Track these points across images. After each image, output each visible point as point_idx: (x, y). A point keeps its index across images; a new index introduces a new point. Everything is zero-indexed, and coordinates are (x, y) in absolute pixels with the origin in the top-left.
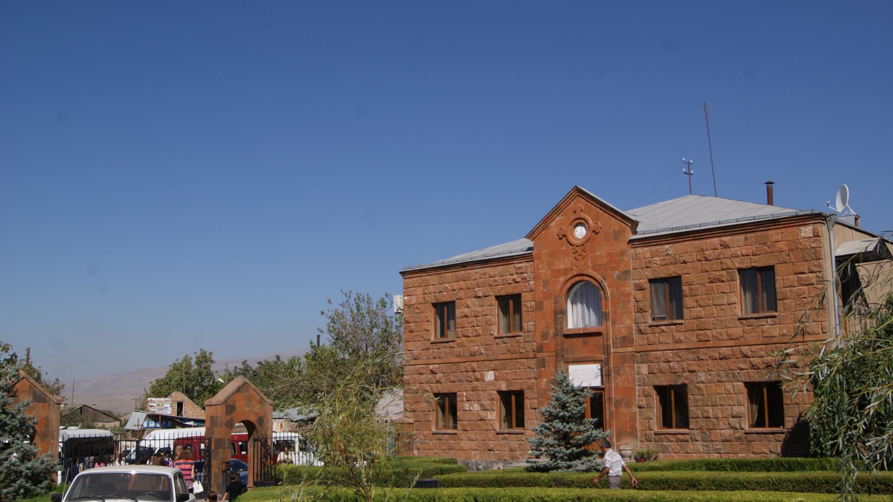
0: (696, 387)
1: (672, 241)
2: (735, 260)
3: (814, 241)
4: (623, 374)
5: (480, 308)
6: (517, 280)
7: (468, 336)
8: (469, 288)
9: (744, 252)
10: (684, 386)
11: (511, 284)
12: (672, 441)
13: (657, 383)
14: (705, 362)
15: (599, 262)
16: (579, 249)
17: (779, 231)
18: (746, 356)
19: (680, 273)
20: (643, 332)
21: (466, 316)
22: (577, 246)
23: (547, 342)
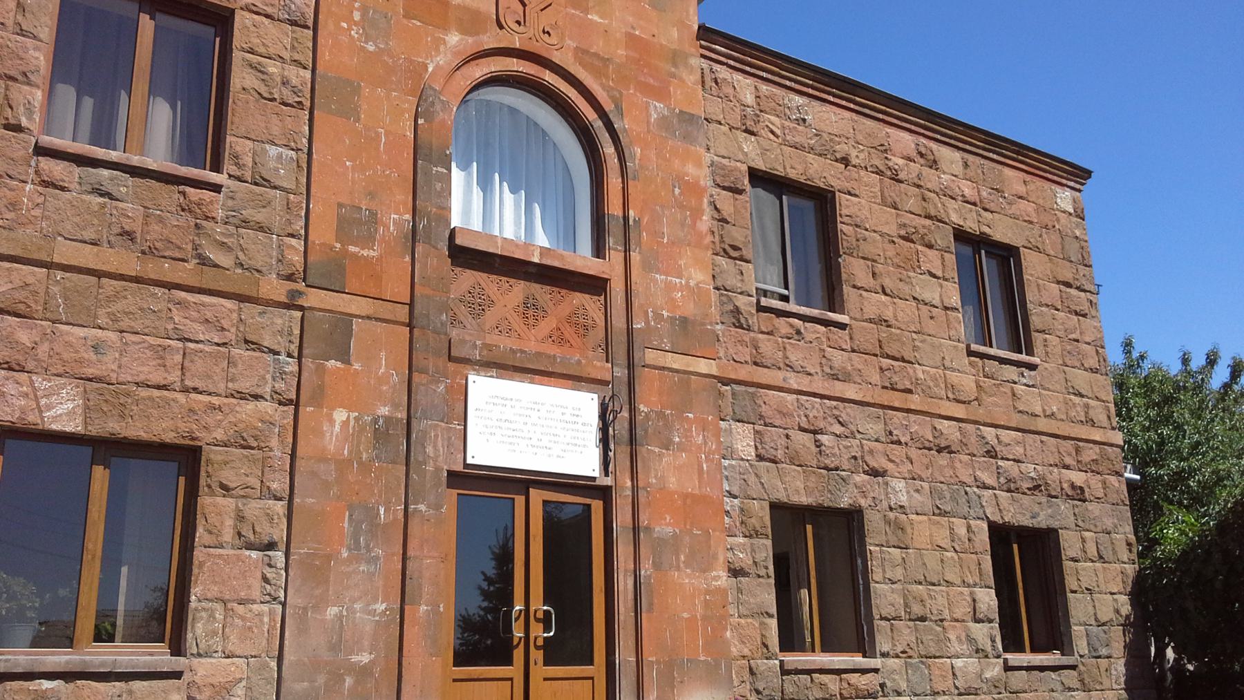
0: (888, 522)
1: (810, 91)
2: (951, 204)
4: (681, 448)
9: (967, 192)
10: (851, 520)
13: (781, 496)
15: (598, 46)
17: (1022, 174)
18: (991, 454)
19: (836, 184)
20: (743, 321)
23: (372, 253)
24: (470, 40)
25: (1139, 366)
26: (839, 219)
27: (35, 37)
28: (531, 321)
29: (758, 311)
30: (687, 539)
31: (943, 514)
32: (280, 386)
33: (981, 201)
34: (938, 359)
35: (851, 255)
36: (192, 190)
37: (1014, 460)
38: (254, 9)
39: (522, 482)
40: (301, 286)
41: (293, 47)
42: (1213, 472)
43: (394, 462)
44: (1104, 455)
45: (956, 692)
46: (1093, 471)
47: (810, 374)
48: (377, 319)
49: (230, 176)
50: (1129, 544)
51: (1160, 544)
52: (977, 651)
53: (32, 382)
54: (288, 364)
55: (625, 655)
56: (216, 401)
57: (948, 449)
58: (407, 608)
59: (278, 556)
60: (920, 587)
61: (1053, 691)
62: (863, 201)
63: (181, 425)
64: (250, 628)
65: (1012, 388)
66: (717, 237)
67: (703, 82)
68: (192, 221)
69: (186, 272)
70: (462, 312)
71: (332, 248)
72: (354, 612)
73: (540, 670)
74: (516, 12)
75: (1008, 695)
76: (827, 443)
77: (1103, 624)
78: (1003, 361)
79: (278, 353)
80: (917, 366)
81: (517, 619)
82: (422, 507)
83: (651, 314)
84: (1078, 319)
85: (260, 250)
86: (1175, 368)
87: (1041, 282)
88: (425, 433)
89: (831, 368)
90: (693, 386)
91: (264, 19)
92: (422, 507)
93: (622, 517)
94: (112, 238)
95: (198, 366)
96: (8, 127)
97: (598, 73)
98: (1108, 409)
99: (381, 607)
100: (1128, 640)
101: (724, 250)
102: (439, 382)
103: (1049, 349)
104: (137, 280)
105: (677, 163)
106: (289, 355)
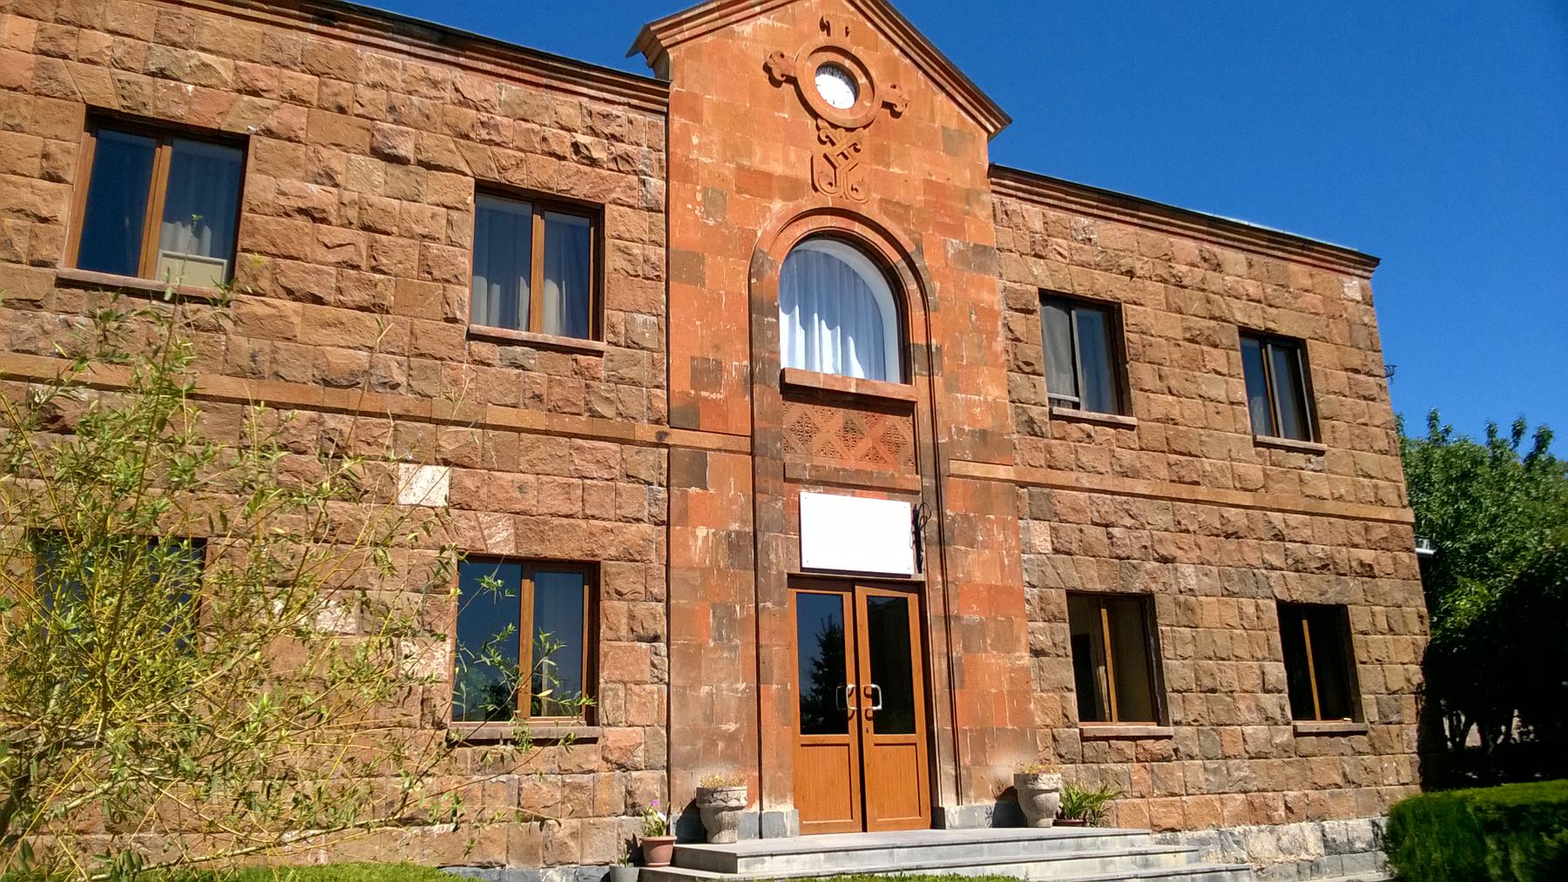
0: (1178, 604)
1: (1095, 211)
2: (1235, 304)
3: (1366, 312)
4: (984, 546)
5: (396, 202)
6: (595, 155)
7: (318, 300)
8: (342, 110)
9: (1252, 291)
10: (1144, 604)
11: (562, 158)
12: (1128, 760)
14: (1192, 537)
15: (900, 195)
16: (843, 141)
17: (1307, 269)
18: (1279, 537)
19: (1121, 295)
20: (1037, 429)
21: (315, 216)
22: (835, 126)
23: (719, 396)
24: (791, 205)
25: (1444, 440)
26: (1125, 327)
27: (461, 246)
28: (851, 443)
29: (1050, 419)
30: (992, 625)
31: (1232, 594)
32: (655, 510)
33: (1266, 298)
34: (1225, 451)
35: (1137, 360)
36: (582, 357)
37: (1302, 542)
38: (620, 202)
39: (848, 581)
40: (666, 428)
41: (651, 230)
42: (1509, 544)
43: (745, 568)
44: (1392, 532)
45: (1247, 756)
46: (1383, 549)
47: (1101, 474)
48: (725, 451)
49: (609, 342)
50: (1421, 617)
51: (1452, 616)
52: (1267, 719)
53: (477, 518)
54: (660, 492)
55: (942, 724)
56: (608, 525)
57: (1235, 535)
58: (762, 686)
59: (662, 646)
60: (1210, 662)
61: (1343, 754)
62: (1149, 309)
63: (585, 545)
64: (645, 703)
65: (1299, 474)
66: (1011, 357)
67: (995, 215)
68: (583, 382)
69: (581, 424)
70: (794, 439)
71: (688, 394)
72: (722, 691)
73: (871, 737)
74: (827, 176)
75: (1298, 758)
76: (1118, 535)
77: (1394, 693)
78: (1289, 449)
79: (651, 484)
80: (1204, 459)
81: (850, 695)
82: (769, 605)
83: (953, 429)
84: (1367, 405)
85: (633, 400)
86: (1481, 440)
87: (1328, 371)
88: (768, 544)
89: (1120, 466)
90: (994, 490)
91: (627, 209)
92: (769, 605)
93: (934, 608)
94: (526, 401)
95: (594, 498)
96: (447, 320)
97: (900, 219)
98: (1398, 488)
99: (742, 686)
100: (1420, 707)
101: (1018, 366)
102: (777, 499)
103: (1336, 435)
104: (547, 433)
105: (972, 292)
106: (661, 485)
